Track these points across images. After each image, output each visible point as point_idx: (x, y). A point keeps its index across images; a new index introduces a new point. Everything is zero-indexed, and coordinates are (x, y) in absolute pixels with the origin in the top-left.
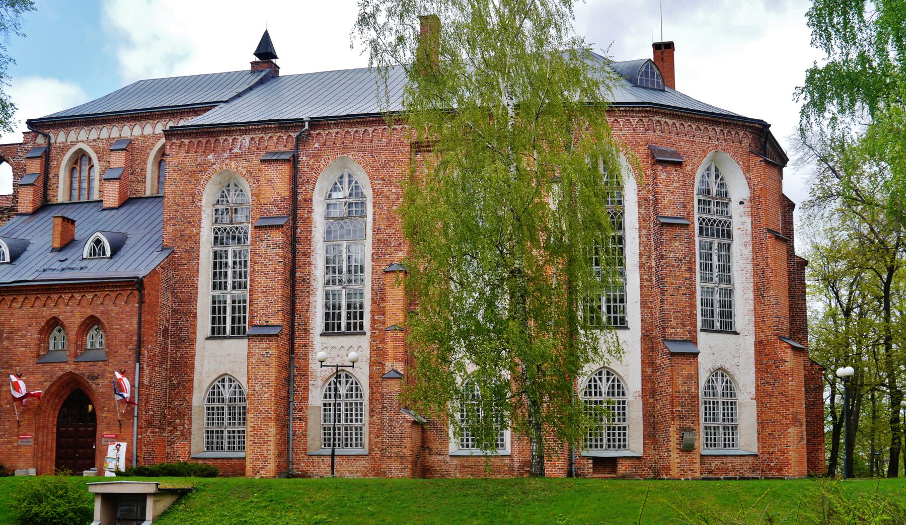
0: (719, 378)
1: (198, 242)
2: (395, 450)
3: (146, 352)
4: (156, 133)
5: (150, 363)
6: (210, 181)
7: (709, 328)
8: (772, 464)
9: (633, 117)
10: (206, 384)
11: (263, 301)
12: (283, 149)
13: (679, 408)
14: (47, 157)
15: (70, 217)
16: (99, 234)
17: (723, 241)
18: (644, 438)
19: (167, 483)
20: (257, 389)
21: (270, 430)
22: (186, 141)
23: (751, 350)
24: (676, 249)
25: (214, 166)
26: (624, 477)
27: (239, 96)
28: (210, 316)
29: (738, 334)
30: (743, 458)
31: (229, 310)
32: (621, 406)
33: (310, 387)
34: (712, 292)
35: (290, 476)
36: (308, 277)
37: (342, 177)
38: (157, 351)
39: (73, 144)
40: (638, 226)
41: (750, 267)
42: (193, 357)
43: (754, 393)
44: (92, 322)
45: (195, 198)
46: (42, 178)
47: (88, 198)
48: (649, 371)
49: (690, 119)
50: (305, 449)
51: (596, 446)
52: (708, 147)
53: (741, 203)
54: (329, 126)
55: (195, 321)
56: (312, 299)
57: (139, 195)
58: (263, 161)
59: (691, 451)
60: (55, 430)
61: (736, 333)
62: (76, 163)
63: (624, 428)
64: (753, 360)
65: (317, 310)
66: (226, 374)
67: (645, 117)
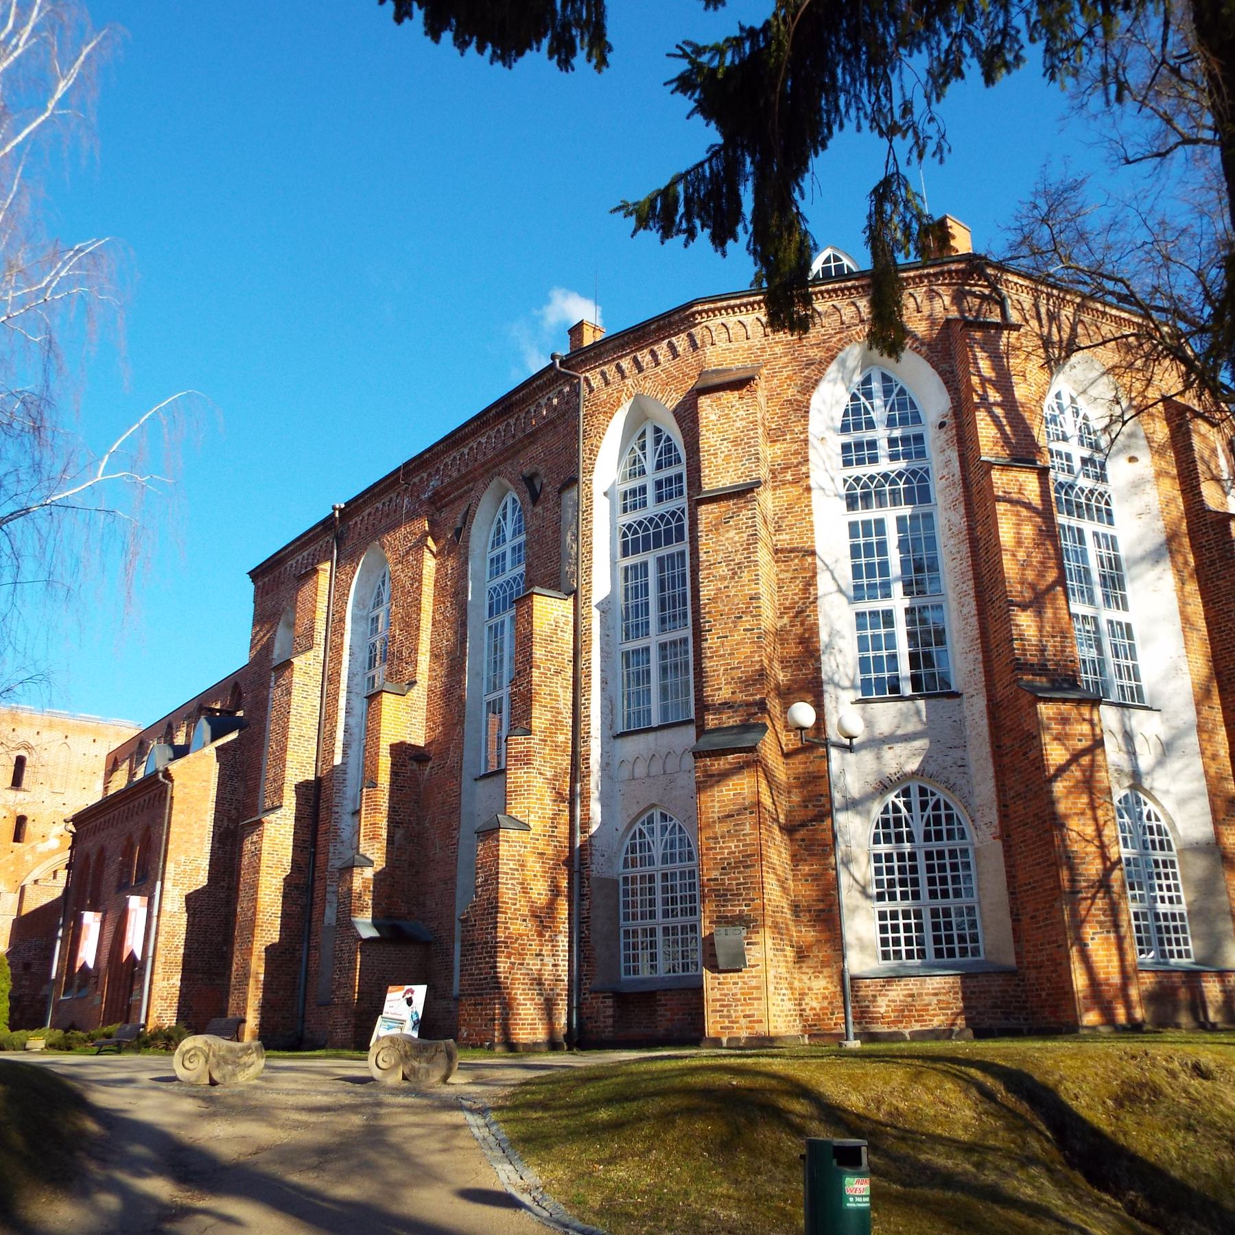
33: (328, 896)
43: (996, 822)
53: (942, 425)
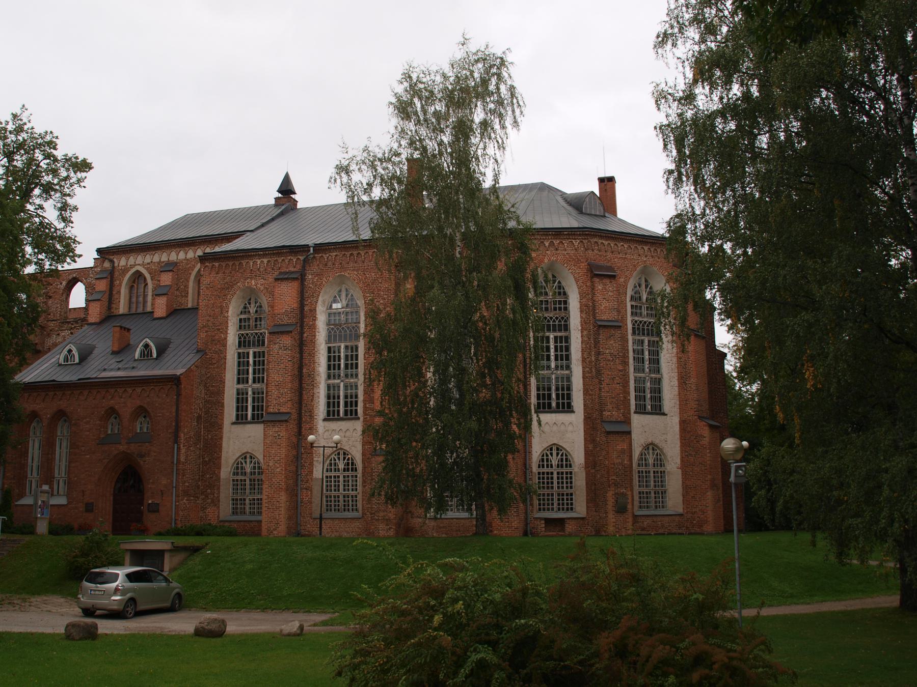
0: (651, 451)
1: (225, 345)
2: (382, 514)
3: (182, 435)
4: (187, 257)
5: (186, 444)
6: (235, 296)
7: (641, 410)
8: (695, 522)
9: (575, 239)
10: (231, 461)
11: (276, 393)
12: (292, 269)
13: (614, 477)
14: (111, 276)
15: (127, 327)
16: (148, 340)
17: (652, 339)
18: (587, 502)
19: (181, 541)
20: (270, 465)
21: (281, 498)
22: (217, 264)
23: (677, 428)
24: (610, 346)
25: (239, 284)
26: (570, 535)
27: (263, 225)
28: (235, 405)
29: (666, 415)
30: (670, 517)
31: (250, 400)
32: (569, 476)
33: (314, 463)
34: (644, 381)
35: (298, 534)
36: (313, 373)
37: (340, 291)
38: (192, 434)
39: (132, 266)
40: (580, 328)
41: (675, 360)
42: (221, 438)
43: (679, 463)
44: (61, 414)
45: (223, 310)
46: (107, 294)
47: (143, 310)
48: (591, 447)
49: (622, 240)
50: (311, 514)
51: (548, 509)
52: (638, 263)
54: (330, 250)
55: (223, 410)
56: (316, 391)
57: (182, 307)
58: (276, 279)
59: (624, 512)
60: (112, 498)
61: (664, 414)
62: (134, 282)
63: (571, 494)
64: (678, 436)
65: (320, 400)
66: (247, 453)
67: (585, 239)
